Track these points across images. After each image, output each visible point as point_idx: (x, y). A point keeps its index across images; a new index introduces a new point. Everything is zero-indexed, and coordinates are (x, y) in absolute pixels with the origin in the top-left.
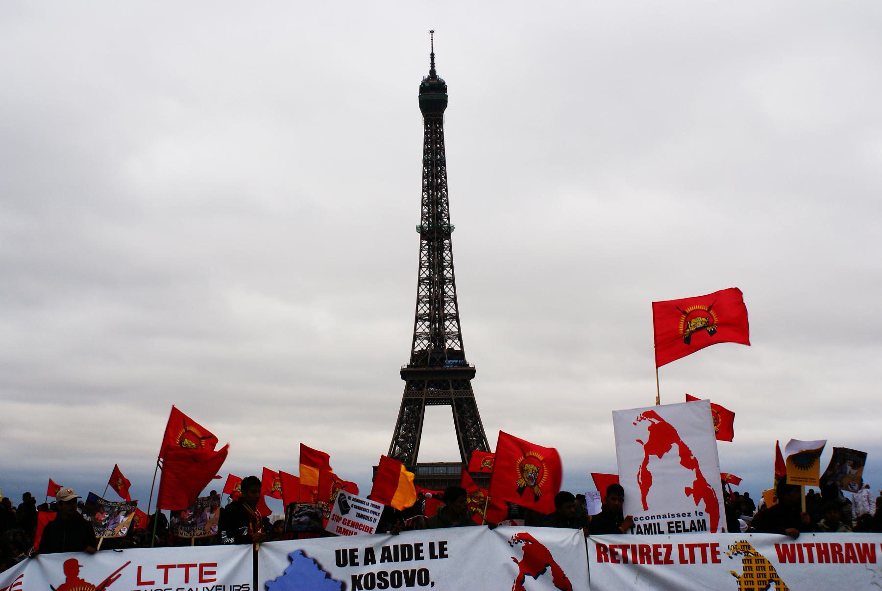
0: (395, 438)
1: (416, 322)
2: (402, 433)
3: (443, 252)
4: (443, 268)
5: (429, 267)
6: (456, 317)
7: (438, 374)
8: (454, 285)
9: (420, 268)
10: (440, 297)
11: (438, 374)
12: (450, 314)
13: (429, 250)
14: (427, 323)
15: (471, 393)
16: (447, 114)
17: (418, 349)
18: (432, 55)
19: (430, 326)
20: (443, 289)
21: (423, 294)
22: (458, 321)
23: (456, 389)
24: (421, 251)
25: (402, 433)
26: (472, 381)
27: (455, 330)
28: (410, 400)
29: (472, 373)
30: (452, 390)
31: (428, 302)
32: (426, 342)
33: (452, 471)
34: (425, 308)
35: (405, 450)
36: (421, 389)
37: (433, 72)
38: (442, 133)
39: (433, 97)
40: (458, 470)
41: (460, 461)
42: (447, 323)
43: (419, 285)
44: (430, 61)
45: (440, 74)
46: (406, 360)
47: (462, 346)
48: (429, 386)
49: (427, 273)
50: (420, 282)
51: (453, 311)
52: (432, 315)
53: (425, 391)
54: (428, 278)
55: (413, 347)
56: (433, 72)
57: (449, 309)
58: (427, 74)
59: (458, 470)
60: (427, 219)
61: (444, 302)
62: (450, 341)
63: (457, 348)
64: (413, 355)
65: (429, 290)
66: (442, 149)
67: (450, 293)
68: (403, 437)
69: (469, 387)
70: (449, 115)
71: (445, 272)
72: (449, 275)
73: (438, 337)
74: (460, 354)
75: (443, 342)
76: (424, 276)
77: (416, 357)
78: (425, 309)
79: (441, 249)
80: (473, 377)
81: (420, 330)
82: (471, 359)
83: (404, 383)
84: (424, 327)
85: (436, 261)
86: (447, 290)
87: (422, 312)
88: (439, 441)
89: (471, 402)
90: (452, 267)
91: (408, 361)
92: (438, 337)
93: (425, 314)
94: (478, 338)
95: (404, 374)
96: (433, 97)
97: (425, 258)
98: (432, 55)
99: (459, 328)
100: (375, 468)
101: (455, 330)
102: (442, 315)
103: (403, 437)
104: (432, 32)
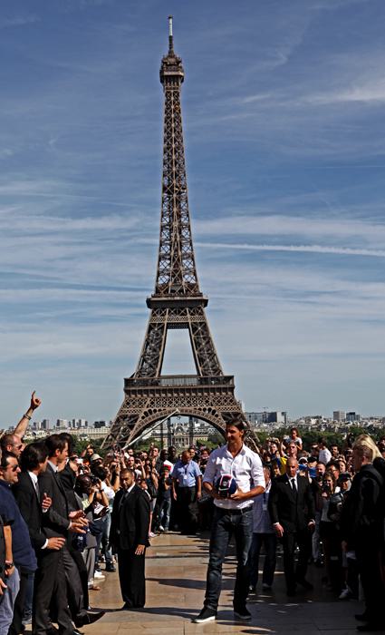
1: (160, 260)
2: (148, 351)
7: (177, 303)
10: (178, 239)
11: (177, 303)
12: (186, 254)
14: (168, 262)
15: (204, 318)
16: (182, 87)
17: (160, 282)
20: (180, 233)
21: (165, 237)
23: (192, 314)
26: (205, 309)
27: (191, 266)
28: (155, 324)
29: (205, 302)
30: (189, 316)
31: (171, 246)
32: (167, 277)
35: (151, 366)
36: (163, 315)
37: (171, 55)
39: (170, 77)
40: (194, 382)
41: (196, 373)
42: (184, 261)
44: (168, 42)
47: (196, 280)
49: (168, 220)
50: (163, 228)
51: (189, 251)
52: (172, 254)
53: (167, 316)
54: (170, 224)
55: (157, 281)
56: (171, 55)
57: (186, 249)
58: (166, 54)
59: (194, 382)
62: (186, 276)
63: (193, 282)
64: (156, 288)
67: (187, 236)
69: (202, 314)
74: (192, 287)
75: (181, 277)
76: (165, 222)
78: (166, 249)
79: (178, 202)
80: (206, 305)
81: (162, 267)
83: (150, 311)
84: (165, 264)
85: (175, 210)
86: (184, 234)
87: (163, 252)
89: (205, 326)
90: (188, 216)
91: (153, 293)
92: (177, 275)
93: (166, 254)
96: (170, 77)
101: (191, 266)
102: (180, 254)
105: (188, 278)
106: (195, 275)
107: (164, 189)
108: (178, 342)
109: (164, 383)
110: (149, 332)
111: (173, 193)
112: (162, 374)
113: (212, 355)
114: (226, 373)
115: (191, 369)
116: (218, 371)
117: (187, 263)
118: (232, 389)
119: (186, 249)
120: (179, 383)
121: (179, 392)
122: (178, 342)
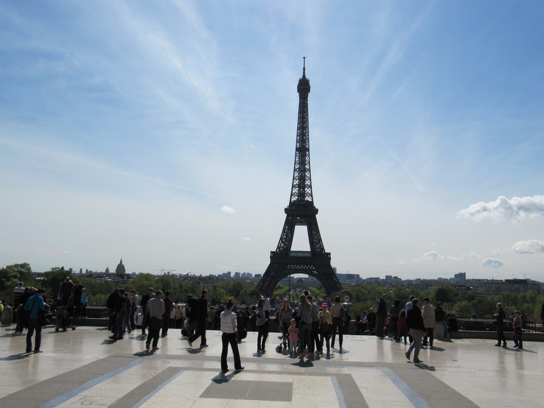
0: (281, 239)
1: (292, 188)
2: (285, 237)
3: (305, 156)
4: (306, 164)
5: (299, 164)
6: (310, 187)
7: (302, 211)
8: (310, 172)
9: (295, 164)
11: (302, 211)
12: (307, 185)
13: (299, 156)
14: (297, 189)
16: (310, 95)
18: (304, 69)
19: (299, 190)
22: (311, 188)
24: (296, 156)
25: (285, 237)
27: (310, 192)
29: (316, 211)
32: (296, 197)
33: (306, 255)
34: (297, 182)
35: (285, 245)
37: (304, 76)
38: (307, 104)
39: (304, 87)
41: (310, 250)
42: (306, 189)
43: (294, 172)
45: (307, 77)
46: (287, 204)
47: (312, 199)
48: (297, 217)
50: (295, 170)
51: (309, 184)
54: (299, 168)
56: (304, 76)
57: (307, 183)
58: (301, 77)
60: (299, 142)
61: (304, 180)
62: (307, 197)
63: (310, 200)
65: (299, 174)
66: (307, 110)
67: (308, 175)
68: (284, 239)
70: (310, 96)
71: (306, 166)
72: (308, 167)
73: (302, 195)
74: (312, 203)
76: (296, 167)
77: (292, 204)
78: (296, 182)
82: (315, 205)
84: (296, 190)
86: (306, 174)
87: (295, 183)
88: (301, 241)
90: (309, 164)
92: (302, 195)
94: (319, 197)
95: (286, 210)
96: (304, 87)
97: (297, 160)
98: (304, 69)
99: (311, 191)
100: (271, 252)
101: (310, 192)
103: (284, 239)
104: (304, 58)
105: (308, 199)
106: (312, 196)
107: (297, 149)
108: (301, 233)
109: (292, 254)
110: (285, 226)
111: (302, 150)
112: (292, 250)
113: (320, 240)
114: (327, 251)
115: (308, 249)
116: (323, 249)
117: (308, 190)
118: (330, 259)
119: (307, 182)
120: (300, 255)
121: (301, 261)
122: (301, 233)
